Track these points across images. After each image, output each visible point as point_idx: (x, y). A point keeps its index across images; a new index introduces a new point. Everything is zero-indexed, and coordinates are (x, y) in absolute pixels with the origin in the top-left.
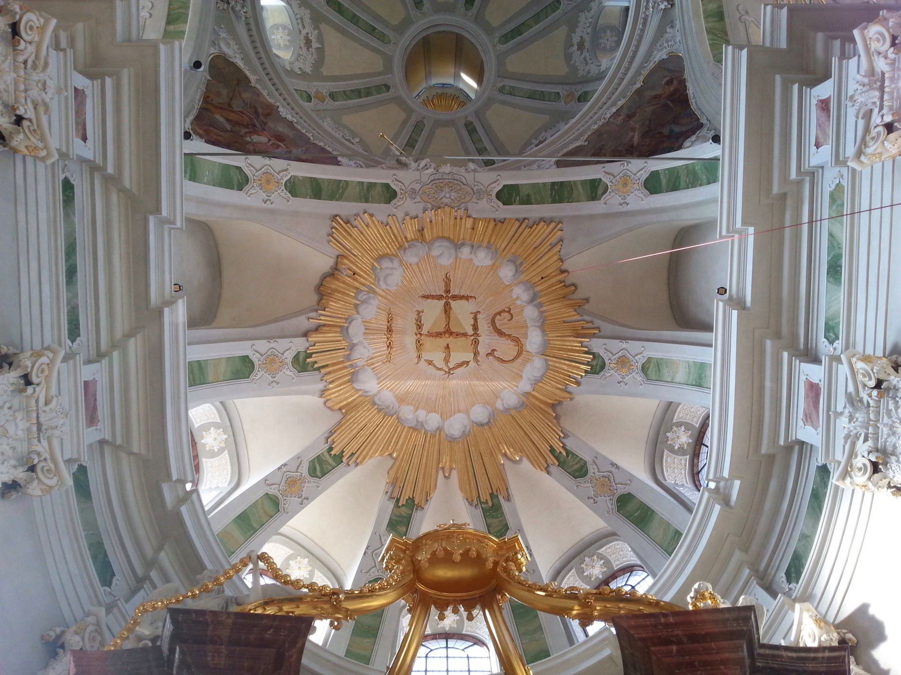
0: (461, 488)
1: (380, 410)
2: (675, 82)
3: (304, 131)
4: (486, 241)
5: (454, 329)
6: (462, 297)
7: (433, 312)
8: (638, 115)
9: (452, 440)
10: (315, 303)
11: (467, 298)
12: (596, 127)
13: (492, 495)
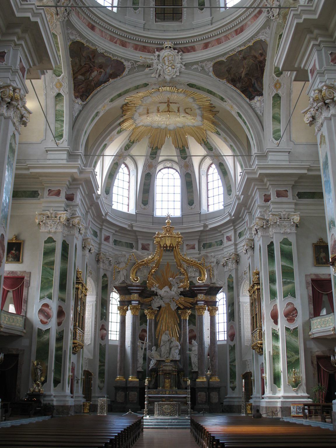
0: (173, 143)
1: (145, 127)
2: (263, 57)
3: (108, 55)
4: (183, 92)
5: (170, 110)
6: (174, 103)
7: (163, 107)
8: (247, 60)
9: (170, 130)
10: (121, 113)
11: (176, 103)
12: (231, 54)
13: (183, 146)
